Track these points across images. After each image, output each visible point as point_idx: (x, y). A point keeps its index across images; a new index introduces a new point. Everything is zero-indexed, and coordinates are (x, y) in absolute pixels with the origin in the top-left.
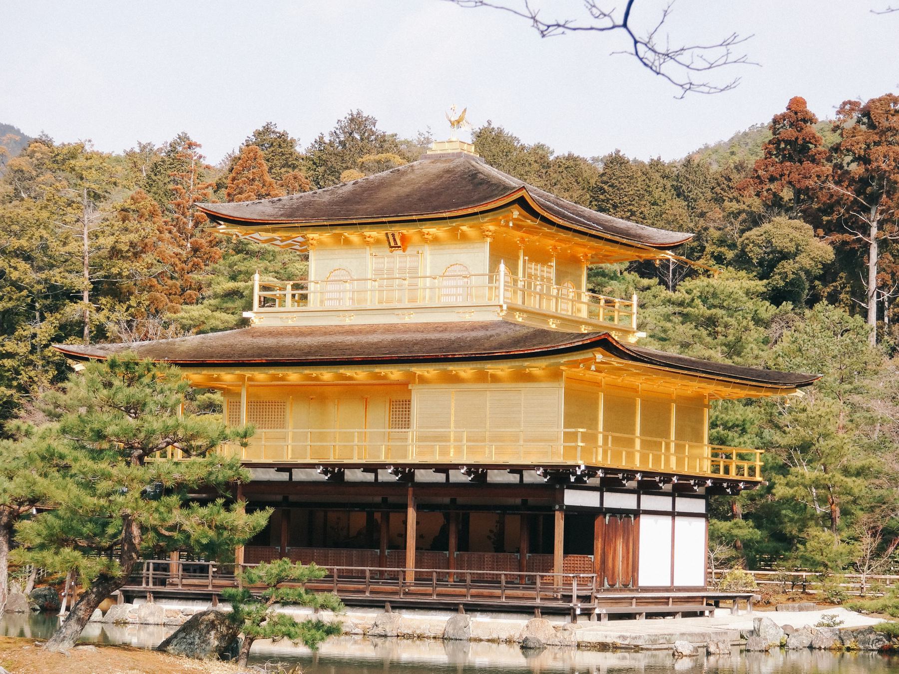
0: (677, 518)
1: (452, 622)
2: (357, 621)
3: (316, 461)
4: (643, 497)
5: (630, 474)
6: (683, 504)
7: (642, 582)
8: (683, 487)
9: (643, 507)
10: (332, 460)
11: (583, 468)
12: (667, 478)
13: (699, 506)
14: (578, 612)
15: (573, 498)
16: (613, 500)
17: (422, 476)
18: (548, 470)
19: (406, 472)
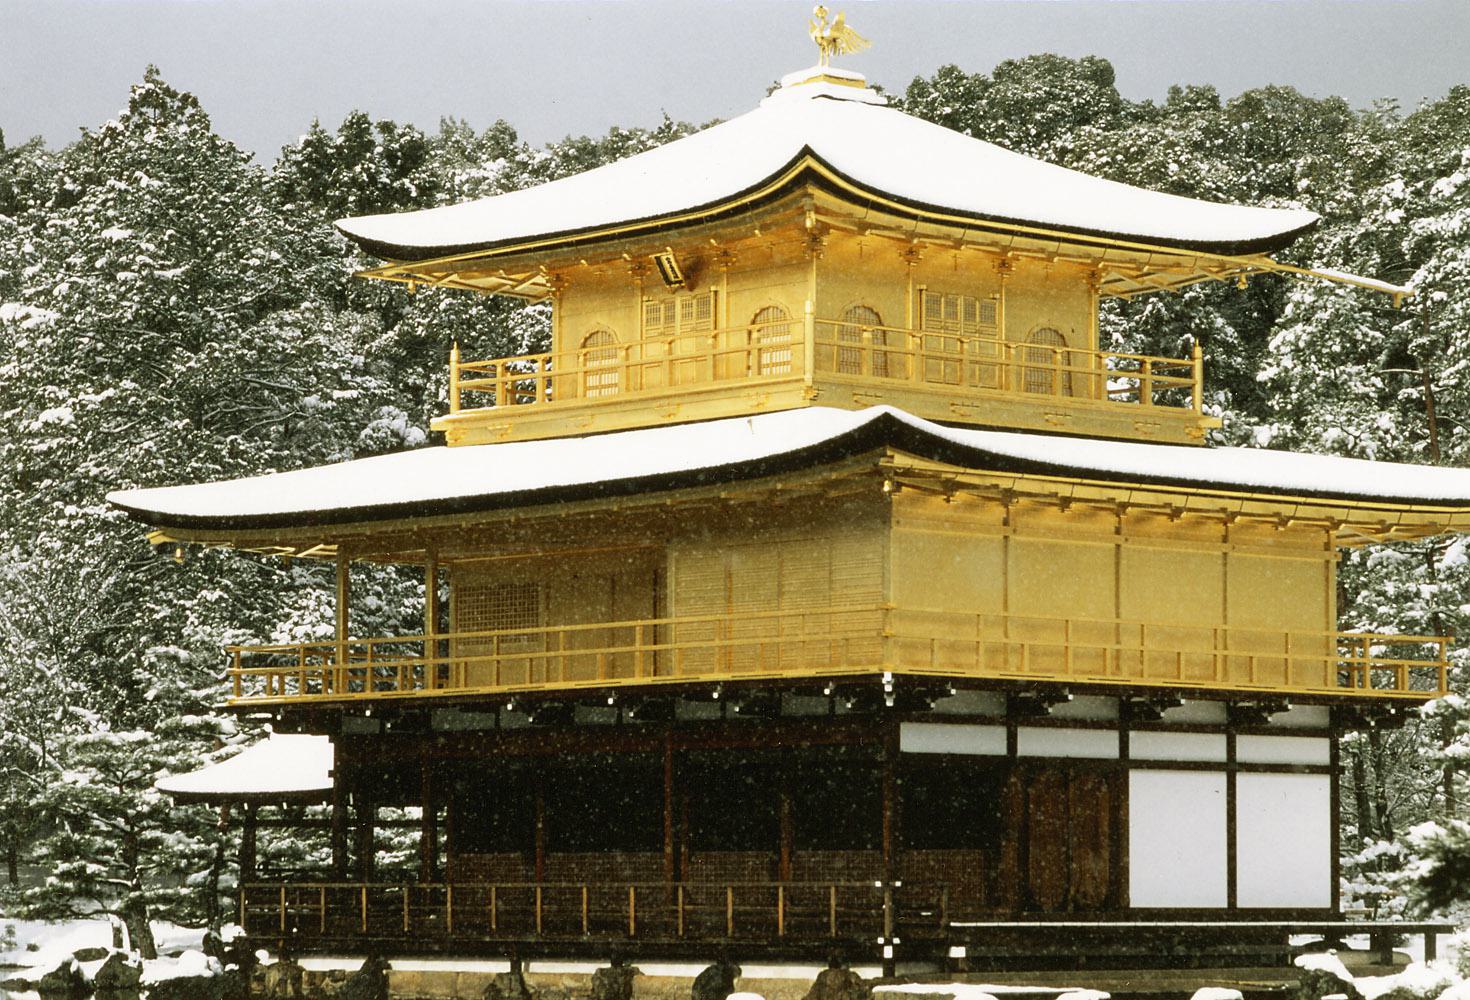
0: (1241, 779)
1: (701, 982)
2: (572, 984)
3: (504, 688)
4: (1132, 734)
5: (1054, 692)
6: (1250, 748)
7: (1141, 895)
8: (1246, 714)
9: (1135, 752)
10: (528, 686)
11: (887, 677)
12: (1167, 697)
13: (1317, 750)
14: (888, 952)
15: (915, 739)
16: (1035, 743)
17: (688, 711)
18: (846, 685)
19: (657, 703)
